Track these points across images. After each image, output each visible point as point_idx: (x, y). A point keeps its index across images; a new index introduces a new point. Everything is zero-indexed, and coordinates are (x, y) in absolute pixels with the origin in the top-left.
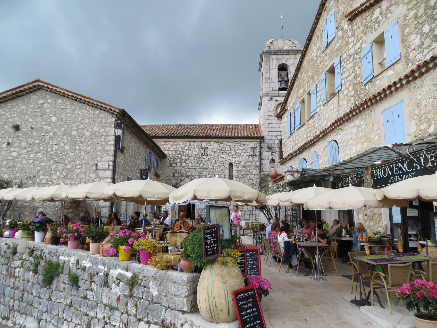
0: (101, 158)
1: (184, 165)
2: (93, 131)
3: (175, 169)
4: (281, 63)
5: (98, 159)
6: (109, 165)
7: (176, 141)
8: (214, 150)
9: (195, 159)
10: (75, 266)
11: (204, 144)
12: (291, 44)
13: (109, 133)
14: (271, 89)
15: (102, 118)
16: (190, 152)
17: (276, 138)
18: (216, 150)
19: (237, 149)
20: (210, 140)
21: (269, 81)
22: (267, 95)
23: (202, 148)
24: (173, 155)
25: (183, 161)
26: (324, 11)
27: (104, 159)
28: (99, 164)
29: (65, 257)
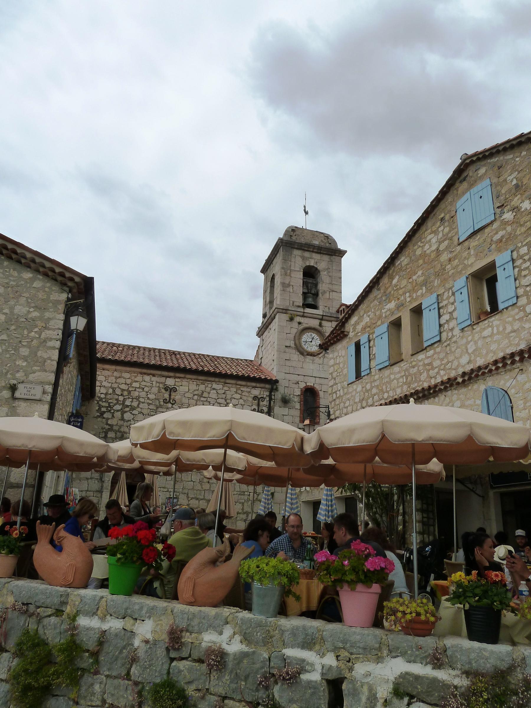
0: (27, 375)
1: (127, 416)
2: (12, 312)
3: (109, 422)
4: (308, 264)
5: (18, 375)
6: (44, 392)
7: (116, 370)
8: (187, 395)
9: (151, 407)
10: (161, 652)
11: (170, 382)
12: (323, 239)
13: (52, 323)
14: (291, 302)
15: (38, 289)
16: (143, 394)
17: (297, 386)
18: (191, 396)
19: (229, 397)
20: (182, 375)
21: (288, 289)
22: (285, 311)
23: (166, 389)
24: (109, 397)
25: (127, 409)
26: (461, 182)
27: (31, 377)
28: (21, 387)
29: (103, 619)
